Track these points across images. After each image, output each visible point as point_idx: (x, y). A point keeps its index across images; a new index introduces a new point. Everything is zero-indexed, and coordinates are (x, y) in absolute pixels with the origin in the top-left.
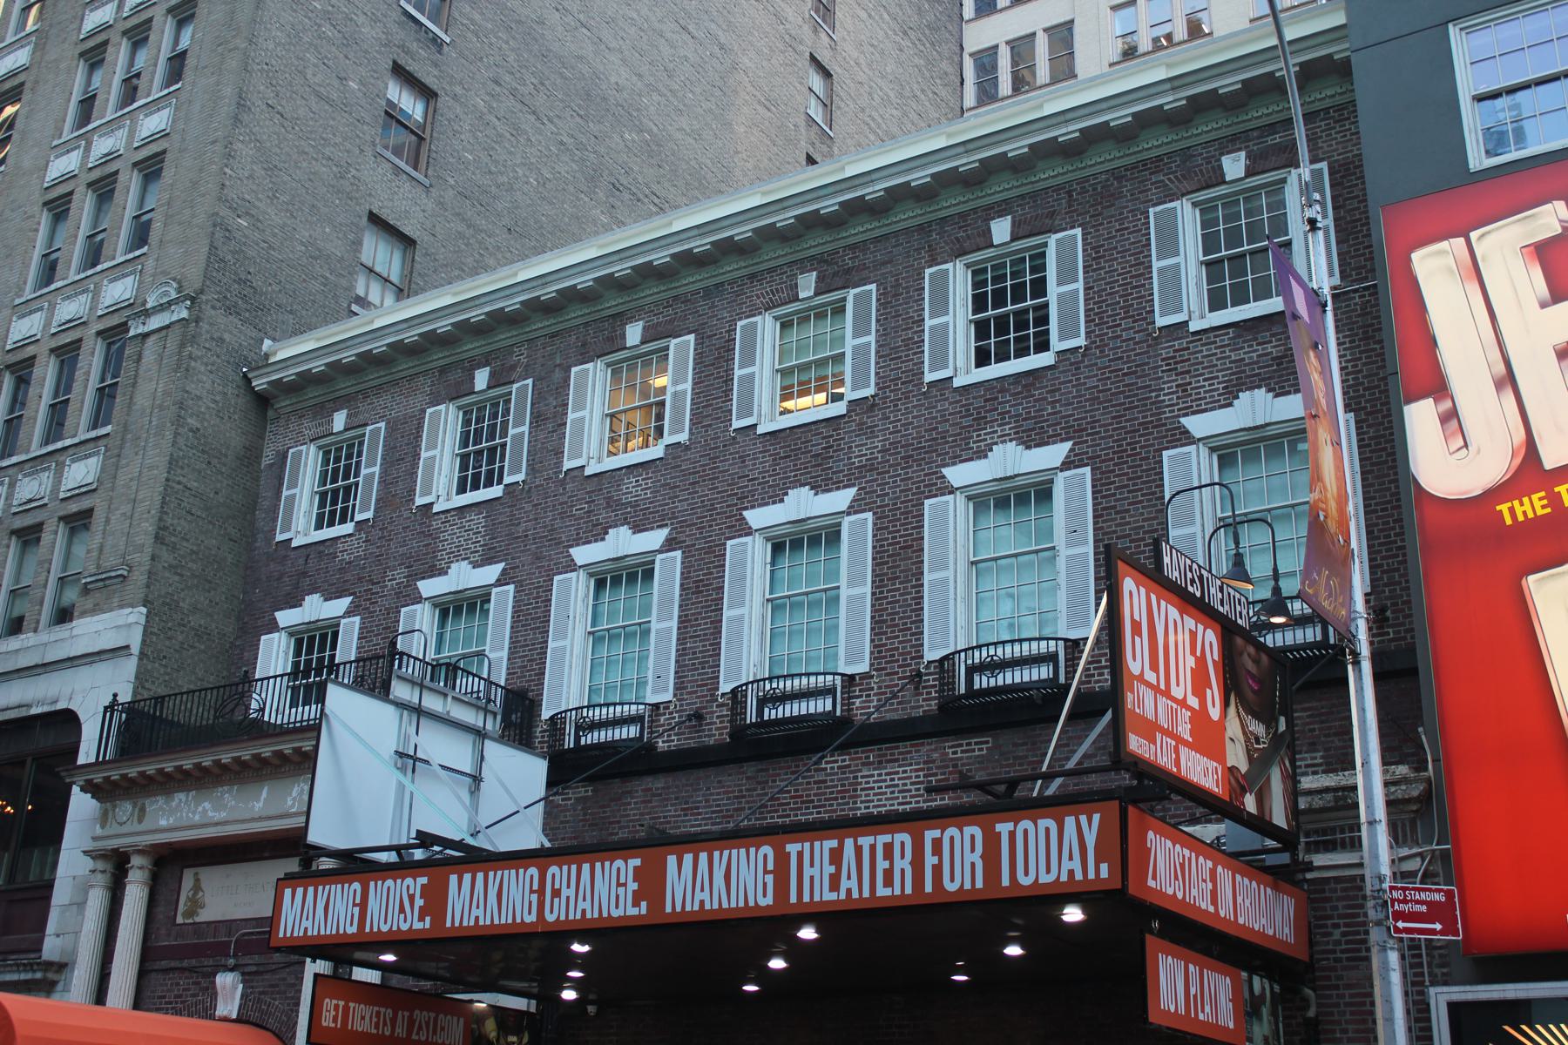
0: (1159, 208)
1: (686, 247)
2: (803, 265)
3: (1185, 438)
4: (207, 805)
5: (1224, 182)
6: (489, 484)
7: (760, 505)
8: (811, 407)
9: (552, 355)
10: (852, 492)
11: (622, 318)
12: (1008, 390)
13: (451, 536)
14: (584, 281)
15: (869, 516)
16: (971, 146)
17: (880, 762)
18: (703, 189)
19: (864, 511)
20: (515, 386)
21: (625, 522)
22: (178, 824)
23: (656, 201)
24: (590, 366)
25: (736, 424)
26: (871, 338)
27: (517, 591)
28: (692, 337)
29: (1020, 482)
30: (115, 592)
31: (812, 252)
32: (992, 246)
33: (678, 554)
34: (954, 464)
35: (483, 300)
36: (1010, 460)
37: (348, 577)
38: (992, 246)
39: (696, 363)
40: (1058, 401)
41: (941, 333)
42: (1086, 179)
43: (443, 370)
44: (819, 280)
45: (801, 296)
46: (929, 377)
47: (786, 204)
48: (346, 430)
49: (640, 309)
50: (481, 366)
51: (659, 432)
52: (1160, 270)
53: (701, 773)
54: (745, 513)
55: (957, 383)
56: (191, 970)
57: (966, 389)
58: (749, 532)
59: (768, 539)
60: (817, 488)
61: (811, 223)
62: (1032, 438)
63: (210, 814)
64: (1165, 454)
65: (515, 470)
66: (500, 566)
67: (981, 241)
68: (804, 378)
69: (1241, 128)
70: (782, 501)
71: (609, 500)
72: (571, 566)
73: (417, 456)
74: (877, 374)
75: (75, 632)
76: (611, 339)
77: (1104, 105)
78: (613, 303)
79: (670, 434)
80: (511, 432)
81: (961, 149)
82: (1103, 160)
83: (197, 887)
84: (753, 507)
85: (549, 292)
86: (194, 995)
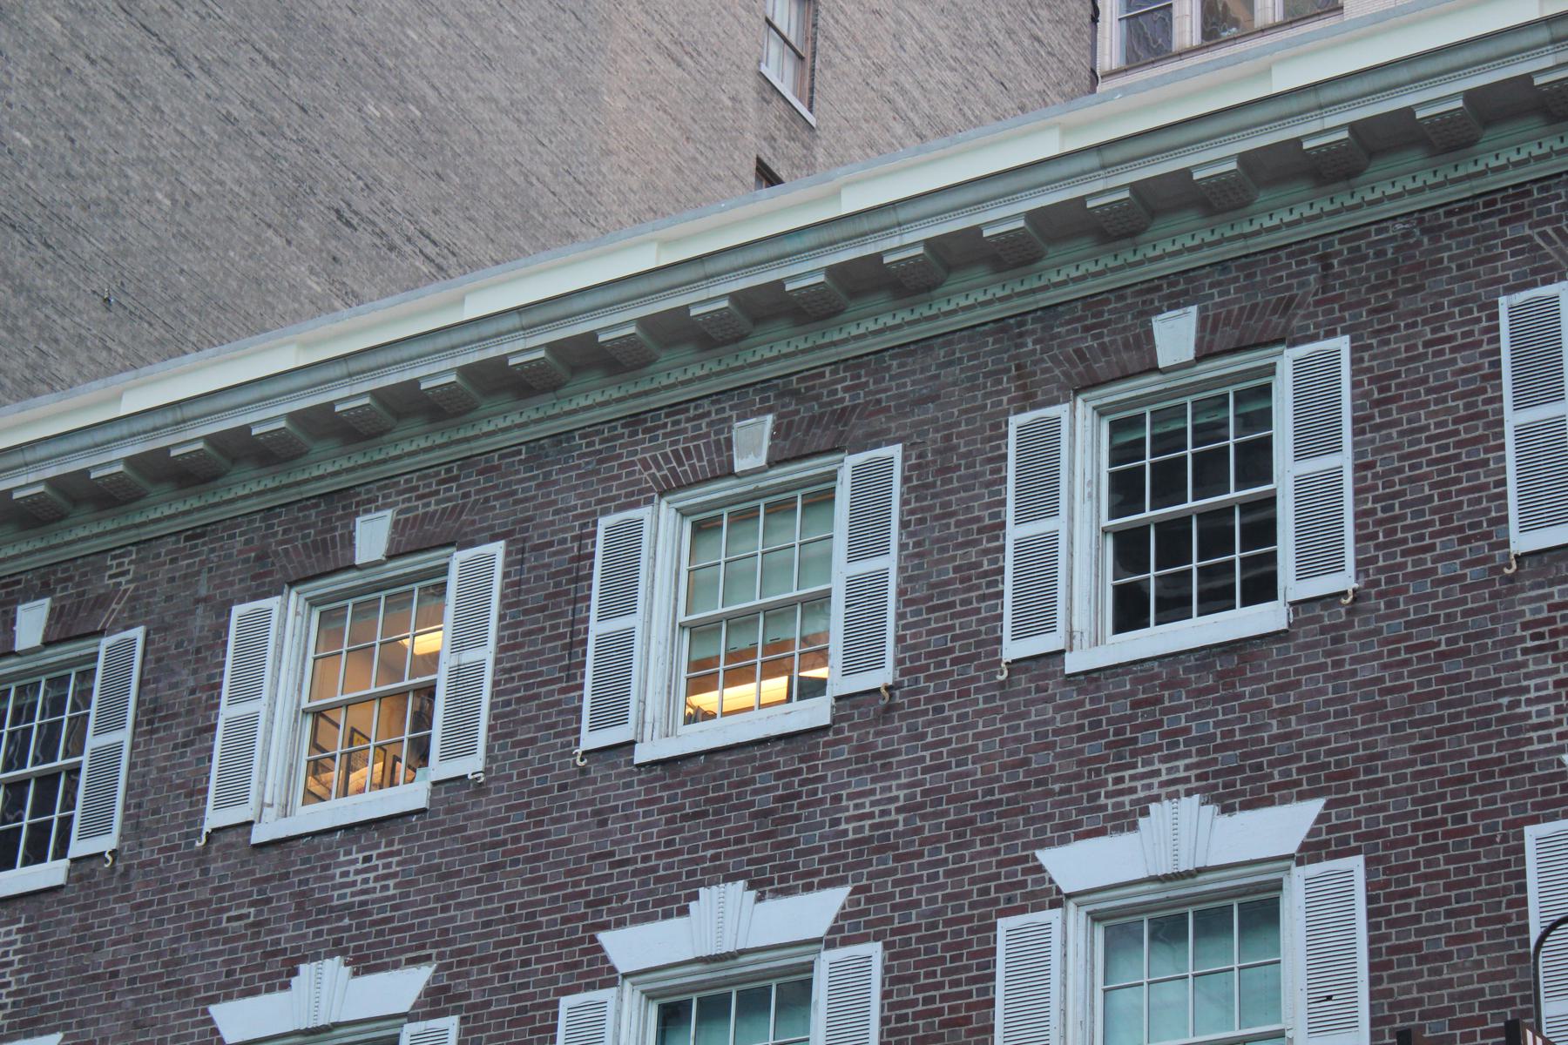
1: (493, 353)
2: (746, 398)
6: (36, 855)
7: (636, 920)
8: (754, 707)
9: (190, 577)
10: (838, 897)
11: (346, 503)
12: (1184, 683)
14: (266, 418)
15: (874, 951)
16: (1112, 155)
18: (530, 229)
20: (106, 642)
21: (337, 949)
23: (430, 250)
24: (274, 603)
25: (591, 740)
26: (889, 562)
28: (498, 549)
31: (767, 372)
32: (1154, 369)
33: (451, 1024)
34: (1064, 841)
35: (42, 452)
36: (1187, 835)
38: (1154, 369)
39: (506, 605)
40: (1296, 709)
41: (1041, 553)
42: (1360, 231)
44: (779, 432)
45: (740, 465)
46: (1013, 649)
47: (711, 267)
50: (30, 595)
51: (421, 752)
52: (1522, 432)
54: (604, 937)
55: (1074, 663)
57: (1091, 676)
58: (606, 976)
59: (650, 996)
60: (765, 885)
61: (767, 309)
62: (1235, 791)
64: (1531, 832)
65: (95, 826)
67: (1131, 359)
68: (742, 643)
70: (684, 911)
74: (900, 639)
76: (322, 547)
77: (1404, 74)
79: (444, 757)
80: (92, 742)
81: (1092, 161)
82: (1401, 188)
84: (620, 924)
85: (188, 440)
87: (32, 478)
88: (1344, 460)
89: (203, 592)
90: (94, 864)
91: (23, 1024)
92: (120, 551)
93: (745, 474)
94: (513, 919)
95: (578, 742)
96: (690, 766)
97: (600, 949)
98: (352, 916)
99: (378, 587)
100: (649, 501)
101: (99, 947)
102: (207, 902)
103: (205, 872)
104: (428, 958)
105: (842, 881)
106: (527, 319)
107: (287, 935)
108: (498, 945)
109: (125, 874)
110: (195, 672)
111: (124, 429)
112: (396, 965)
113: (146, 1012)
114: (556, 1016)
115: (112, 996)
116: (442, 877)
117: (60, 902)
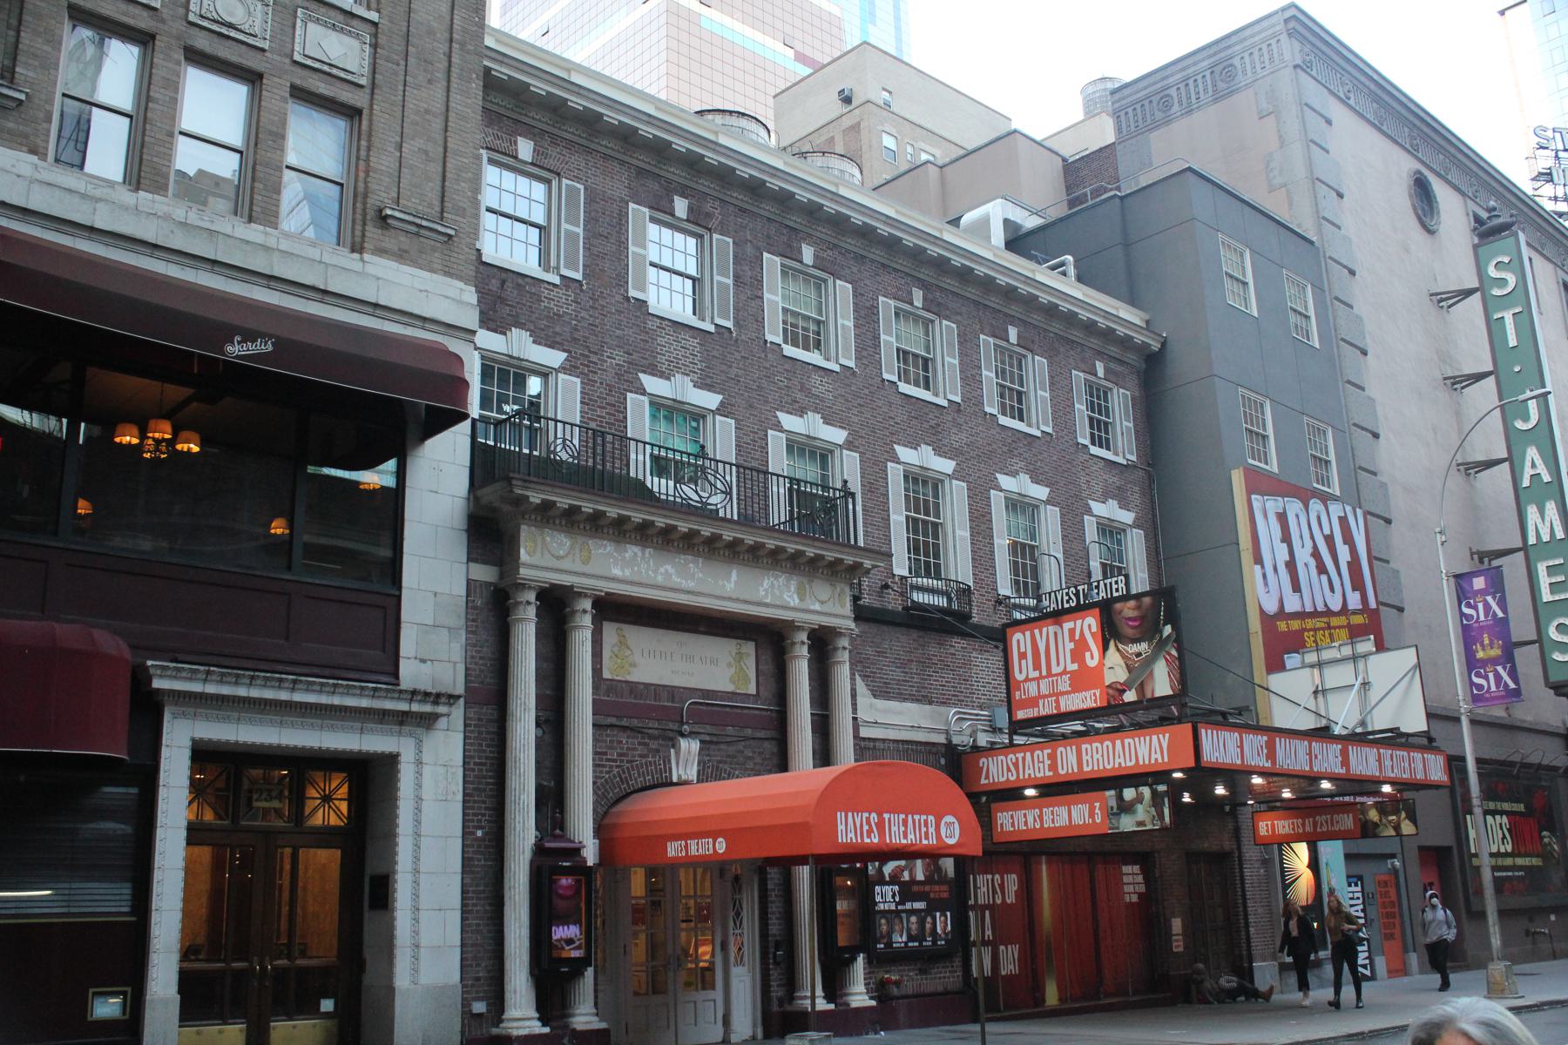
2: (924, 285)
3: (1089, 511)
4: (669, 567)
13: (667, 343)
21: (816, 411)
22: (636, 579)
26: (956, 362)
30: (434, 250)
37: (558, 329)
43: (641, 172)
44: (925, 299)
48: (532, 164)
53: (885, 628)
56: (632, 729)
61: (941, 264)
71: (802, 385)
72: (778, 427)
73: (622, 245)
75: (370, 269)
83: (623, 643)
86: (641, 756)
107: (799, 396)
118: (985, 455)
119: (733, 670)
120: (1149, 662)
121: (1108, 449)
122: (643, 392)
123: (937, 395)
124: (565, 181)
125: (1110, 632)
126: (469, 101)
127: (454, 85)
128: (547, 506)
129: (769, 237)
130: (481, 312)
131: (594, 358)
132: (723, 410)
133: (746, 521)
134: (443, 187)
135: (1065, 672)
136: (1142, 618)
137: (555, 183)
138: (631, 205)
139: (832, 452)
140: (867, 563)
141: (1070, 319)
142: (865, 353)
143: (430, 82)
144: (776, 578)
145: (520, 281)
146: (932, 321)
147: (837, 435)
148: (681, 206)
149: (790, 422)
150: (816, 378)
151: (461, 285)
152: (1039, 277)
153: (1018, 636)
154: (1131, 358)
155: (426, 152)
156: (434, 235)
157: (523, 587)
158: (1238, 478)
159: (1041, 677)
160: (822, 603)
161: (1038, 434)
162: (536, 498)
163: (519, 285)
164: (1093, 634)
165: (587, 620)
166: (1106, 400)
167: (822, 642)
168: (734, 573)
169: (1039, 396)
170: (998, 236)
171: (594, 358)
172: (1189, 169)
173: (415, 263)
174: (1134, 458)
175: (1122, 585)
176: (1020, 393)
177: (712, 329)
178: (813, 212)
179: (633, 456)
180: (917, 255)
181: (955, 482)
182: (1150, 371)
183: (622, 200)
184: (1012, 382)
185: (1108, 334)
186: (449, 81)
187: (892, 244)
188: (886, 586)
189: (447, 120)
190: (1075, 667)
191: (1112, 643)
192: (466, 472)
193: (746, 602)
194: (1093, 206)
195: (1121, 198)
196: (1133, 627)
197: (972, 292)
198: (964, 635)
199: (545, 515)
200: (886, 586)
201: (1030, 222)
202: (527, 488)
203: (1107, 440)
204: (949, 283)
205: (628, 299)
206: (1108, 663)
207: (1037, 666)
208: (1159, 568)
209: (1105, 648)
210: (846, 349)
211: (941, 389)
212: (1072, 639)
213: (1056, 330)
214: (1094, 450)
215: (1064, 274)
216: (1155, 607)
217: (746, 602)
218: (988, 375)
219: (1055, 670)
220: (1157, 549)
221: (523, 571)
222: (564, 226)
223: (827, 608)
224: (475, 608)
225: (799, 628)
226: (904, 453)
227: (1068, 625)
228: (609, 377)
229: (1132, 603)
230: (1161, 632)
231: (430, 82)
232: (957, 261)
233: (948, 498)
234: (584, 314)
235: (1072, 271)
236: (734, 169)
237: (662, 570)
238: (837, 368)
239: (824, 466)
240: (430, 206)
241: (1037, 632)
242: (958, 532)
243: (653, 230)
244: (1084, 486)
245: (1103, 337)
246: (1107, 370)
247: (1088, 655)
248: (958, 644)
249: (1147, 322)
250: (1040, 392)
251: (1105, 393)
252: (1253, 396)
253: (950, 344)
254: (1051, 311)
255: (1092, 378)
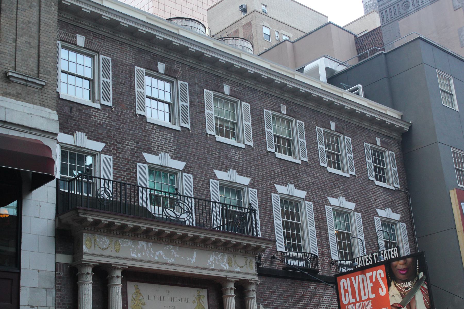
0: (366, 144)
2: (286, 103)
4: (161, 252)
5: (376, 145)
17: (324, 289)
19: (309, 201)
20: (180, 82)
21: (234, 169)
22: (144, 259)
26: (304, 141)
27: (193, 179)
29: (344, 210)
30: (35, 93)
37: (100, 131)
42: (349, 123)
43: (140, 51)
44: (287, 109)
45: (283, 112)
48: (84, 48)
49: (228, 80)
53: (274, 279)
54: (275, 185)
58: (277, 193)
63: (163, 257)
66: (185, 163)
69: (379, 132)
70: (286, 186)
72: (215, 177)
73: (132, 88)
78: (220, 72)
81: (337, 97)
83: (138, 293)
87: (178, 42)
88: (352, 156)
89: (196, 82)
90: (185, 129)
91: (177, 157)
92: (179, 63)
93: (283, 114)
94: (261, 176)
95: (266, 148)
96: (283, 161)
97: (275, 187)
98: (236, 163)
99: (224, 98)
100: (270, 110)
101: (189, 148)
102: (209, 148)
103: (207, 142)
104: (249, 177)
105: (305, 190)
106: (267, 71)
108: (260, 179)
109: (192, 134)
110: (198, 98)
111: (198, 44)
112: (244, 176)
113: (202, 165)
114: (271, 196)
115: (194, 159)
116: (249, 163)
117: (180, 134)
118: (320, 189)
119: (196, 305)
120: (413, 292)
121: (385, 182)
122: (145, 162)
123: (295, 158)
124: (102, 56)
125: (391, 277)
126: (51, 16)
127: (42, 9)
128: (97, 222)
129: (206, 81)
130: (60, 124)
131: (119, 146)
132: (186, 170)
133: (200, 226)
134: (39, 60)
135: (369, 299)
136: (407, 269)
137: (96, 57)
138: (136, 68)
139: (243, 189)
140: (263, 246)
141: (362, 116)
142: (258, 138)
143: (30, 7)
144: (217, 255)
145: (80, 107)
146: (291, 121)
147: (245, 181)
148: (161, 67)
149: (220, 174)
150: (233, 152)
151: (49, 110)
152: (345, 96)
153: (343, 281)
154: (394, 135)
155: (29, 43)
156: (34, 85)
157: (85, 265)
158: (453, 194)
159: (356, 302)
160: (241, 267)
161: (348, 176)
162: (91, 219)
163: (80, 110)
164: (382, 278)
165: (119, 282)
166: (382, 157)
167: (242, 288)
168: (195, 253)
169: (348, 156)
170: (323, 76)
171: (119, 146)
172: (420, 38)
173: (25, 100)
174: (398, 186)
175: (396, 252)
176: (338, 156)
177: (179, 129)
178: (228, 67)
179: (140, 195)
180: (282, 87)
181: (306, 202)
182: (404, 141)
183: (131, 65)
184: (334, 150)
185: (382, 124)
186: (40, 7)
187: (269, 82)
188: (274, 257)
189: (39, 27)
190: (374, 296)
191: (392, 283)
192: (54, 207)
193: (202, 268)
194: (371, 59)
195: (385, 54)
196: (403, 274)
197: (311, 105)
198: (315, 281)
199: (96, 227)
200: (274, 257)
201: (339, 68)
202: (86, 214)
203: (384, 177)
204: (299, 101)
205: (136, 115)
206: (391, 293)
207: (354, 296)
208: (415, 242)
209: (389, 286)
210: (248, 137)
211: (297, 155)
212: (371, 281)
213: (356, 123)
214: (378, 183)
215: (358, 94)
216: (414, 263)
217: (202, 268)
218: (321, 146)
219: (364, 298)
220: (413, 232)
221: (85, 257)
222: (102, 79)
223: (244, 270)
224: (60, 277)
225: (229, 281)
226: (279, 188)
227: (369, 274)
228: (127, 155)
229: (402, 262)
230: (418, 276)
231: (30, 7)
232: (303, 89)
233: (303, 210)
234: (113, 123)
235: (361, 92)
236: (188, 48)
237: (157, 254)
238: (243, 146)
239: (239, 197)
240: (32, 70)
241: (353, 278)
242: (309, 228)
243: (147, 80)
244: (373, 202)
245: (379, 125)
246: (382, 142)
247: (380, 289)
248: (312, 286)
249: (402, 116)
250: (348, 155)
251: (382, 154)
252: (459, 152)
253: (301, 132)
254: (352, 113)
255: (375, 146)
